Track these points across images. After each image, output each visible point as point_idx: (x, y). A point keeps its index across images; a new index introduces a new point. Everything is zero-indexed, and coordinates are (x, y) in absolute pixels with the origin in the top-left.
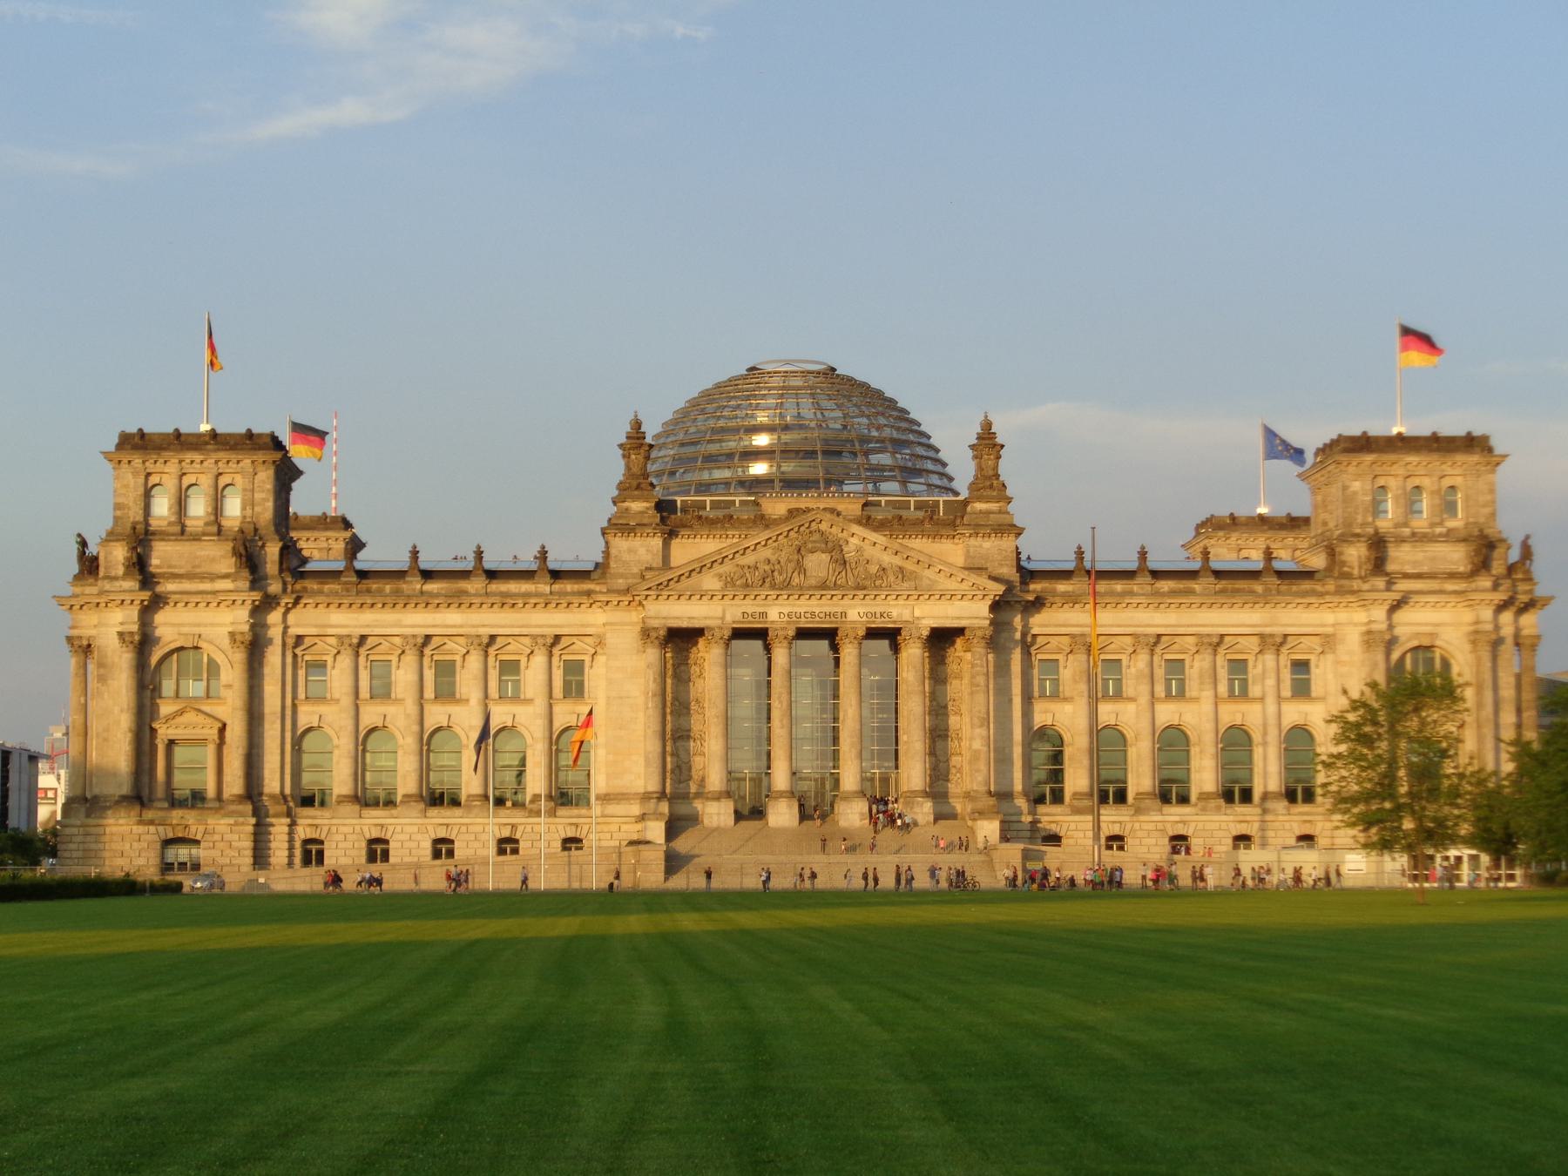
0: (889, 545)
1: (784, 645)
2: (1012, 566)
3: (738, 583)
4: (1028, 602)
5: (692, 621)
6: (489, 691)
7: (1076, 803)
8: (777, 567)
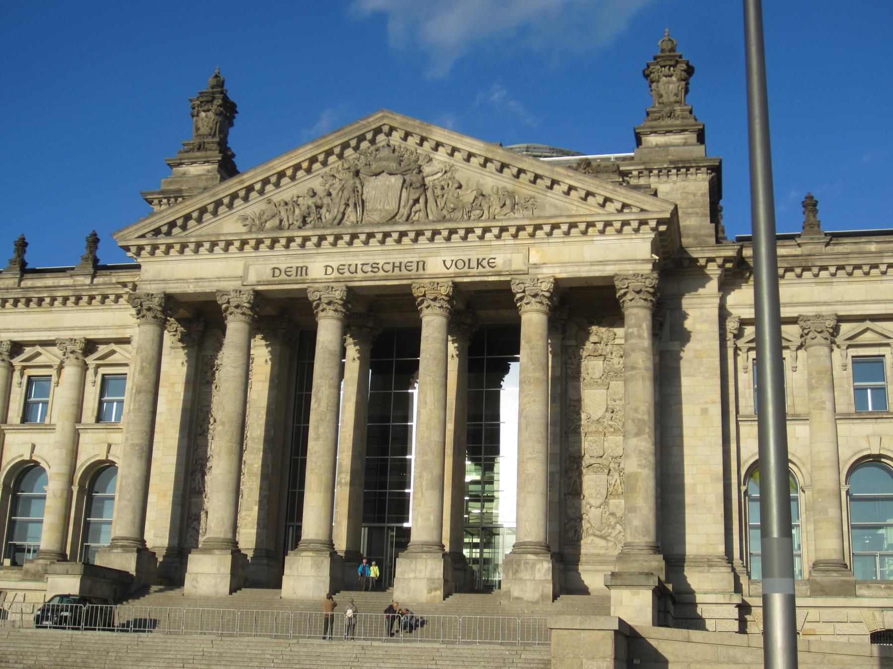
0: (490, 156)
1: (331, 313)
2: (704, 215)
3: (268, 225)
4: (727, 260)
5: (200, 284)
6: (10, 414)
7: (818, 577)
8: (326, 200)
